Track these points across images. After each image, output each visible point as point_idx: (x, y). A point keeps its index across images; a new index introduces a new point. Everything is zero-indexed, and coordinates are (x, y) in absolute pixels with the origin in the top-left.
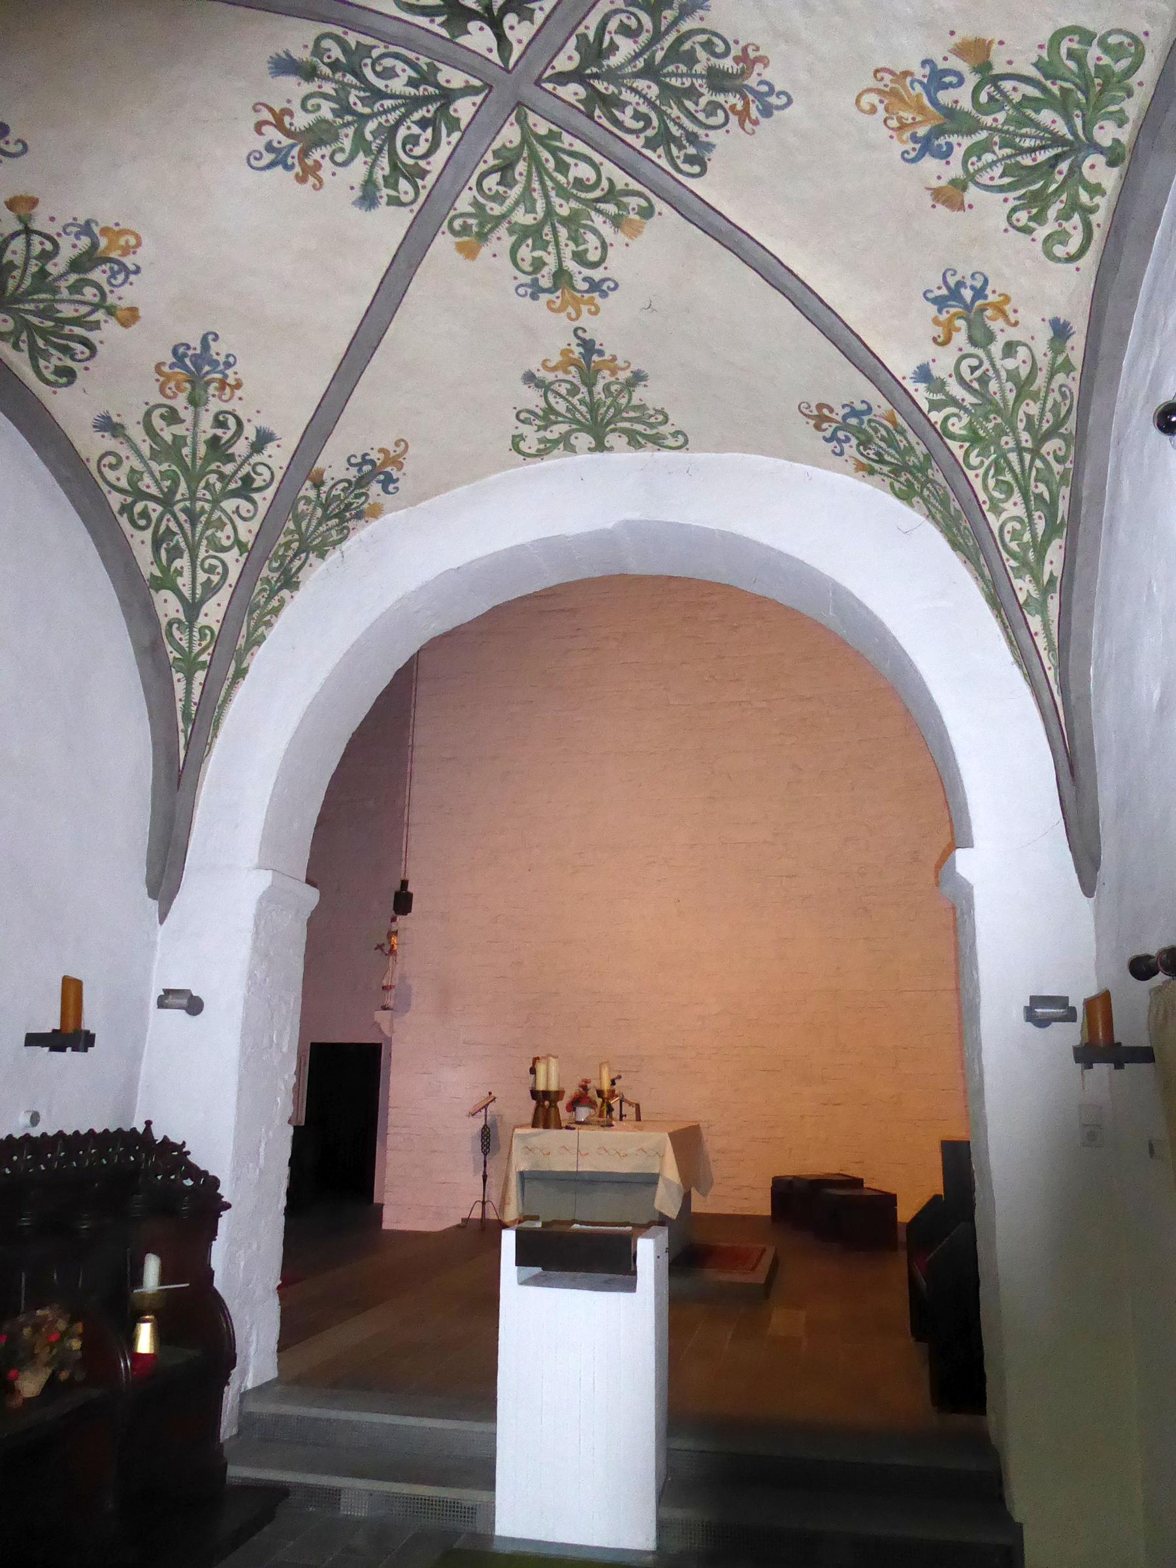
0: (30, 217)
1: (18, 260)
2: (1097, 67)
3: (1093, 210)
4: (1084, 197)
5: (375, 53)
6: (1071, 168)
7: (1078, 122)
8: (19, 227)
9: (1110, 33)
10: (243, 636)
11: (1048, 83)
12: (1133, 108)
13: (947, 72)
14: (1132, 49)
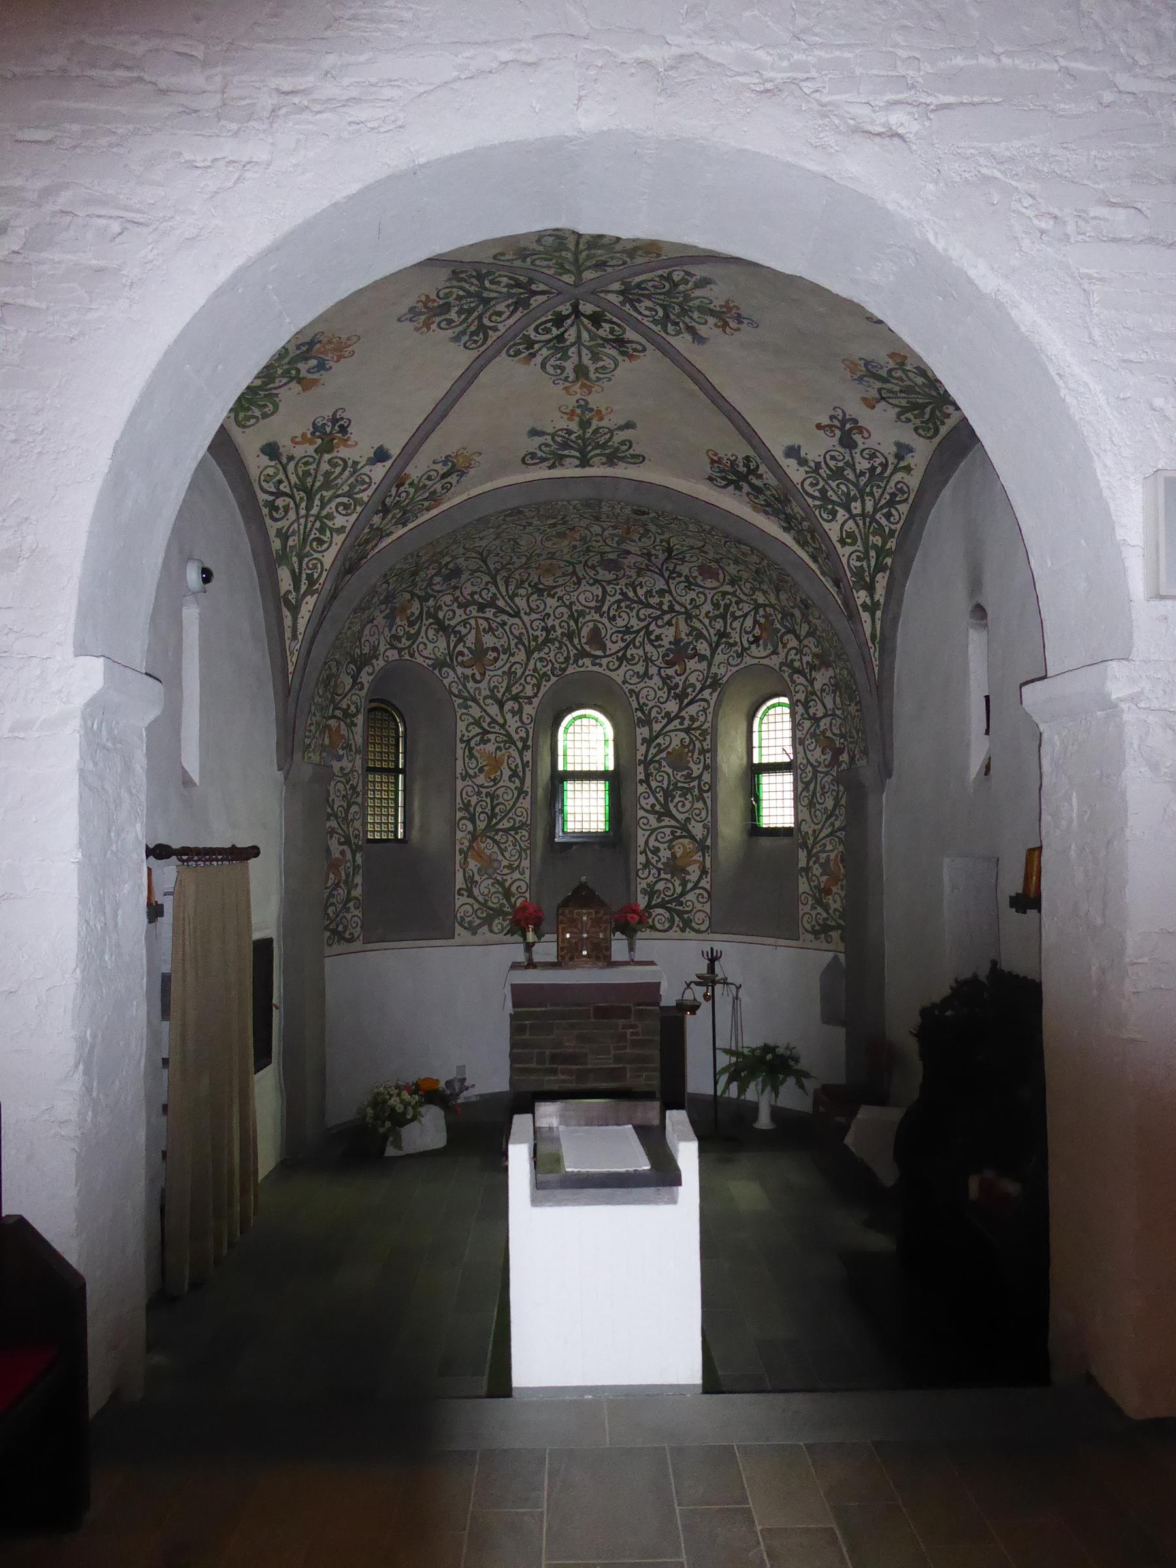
5: (651, 319)
13: (318, 371)
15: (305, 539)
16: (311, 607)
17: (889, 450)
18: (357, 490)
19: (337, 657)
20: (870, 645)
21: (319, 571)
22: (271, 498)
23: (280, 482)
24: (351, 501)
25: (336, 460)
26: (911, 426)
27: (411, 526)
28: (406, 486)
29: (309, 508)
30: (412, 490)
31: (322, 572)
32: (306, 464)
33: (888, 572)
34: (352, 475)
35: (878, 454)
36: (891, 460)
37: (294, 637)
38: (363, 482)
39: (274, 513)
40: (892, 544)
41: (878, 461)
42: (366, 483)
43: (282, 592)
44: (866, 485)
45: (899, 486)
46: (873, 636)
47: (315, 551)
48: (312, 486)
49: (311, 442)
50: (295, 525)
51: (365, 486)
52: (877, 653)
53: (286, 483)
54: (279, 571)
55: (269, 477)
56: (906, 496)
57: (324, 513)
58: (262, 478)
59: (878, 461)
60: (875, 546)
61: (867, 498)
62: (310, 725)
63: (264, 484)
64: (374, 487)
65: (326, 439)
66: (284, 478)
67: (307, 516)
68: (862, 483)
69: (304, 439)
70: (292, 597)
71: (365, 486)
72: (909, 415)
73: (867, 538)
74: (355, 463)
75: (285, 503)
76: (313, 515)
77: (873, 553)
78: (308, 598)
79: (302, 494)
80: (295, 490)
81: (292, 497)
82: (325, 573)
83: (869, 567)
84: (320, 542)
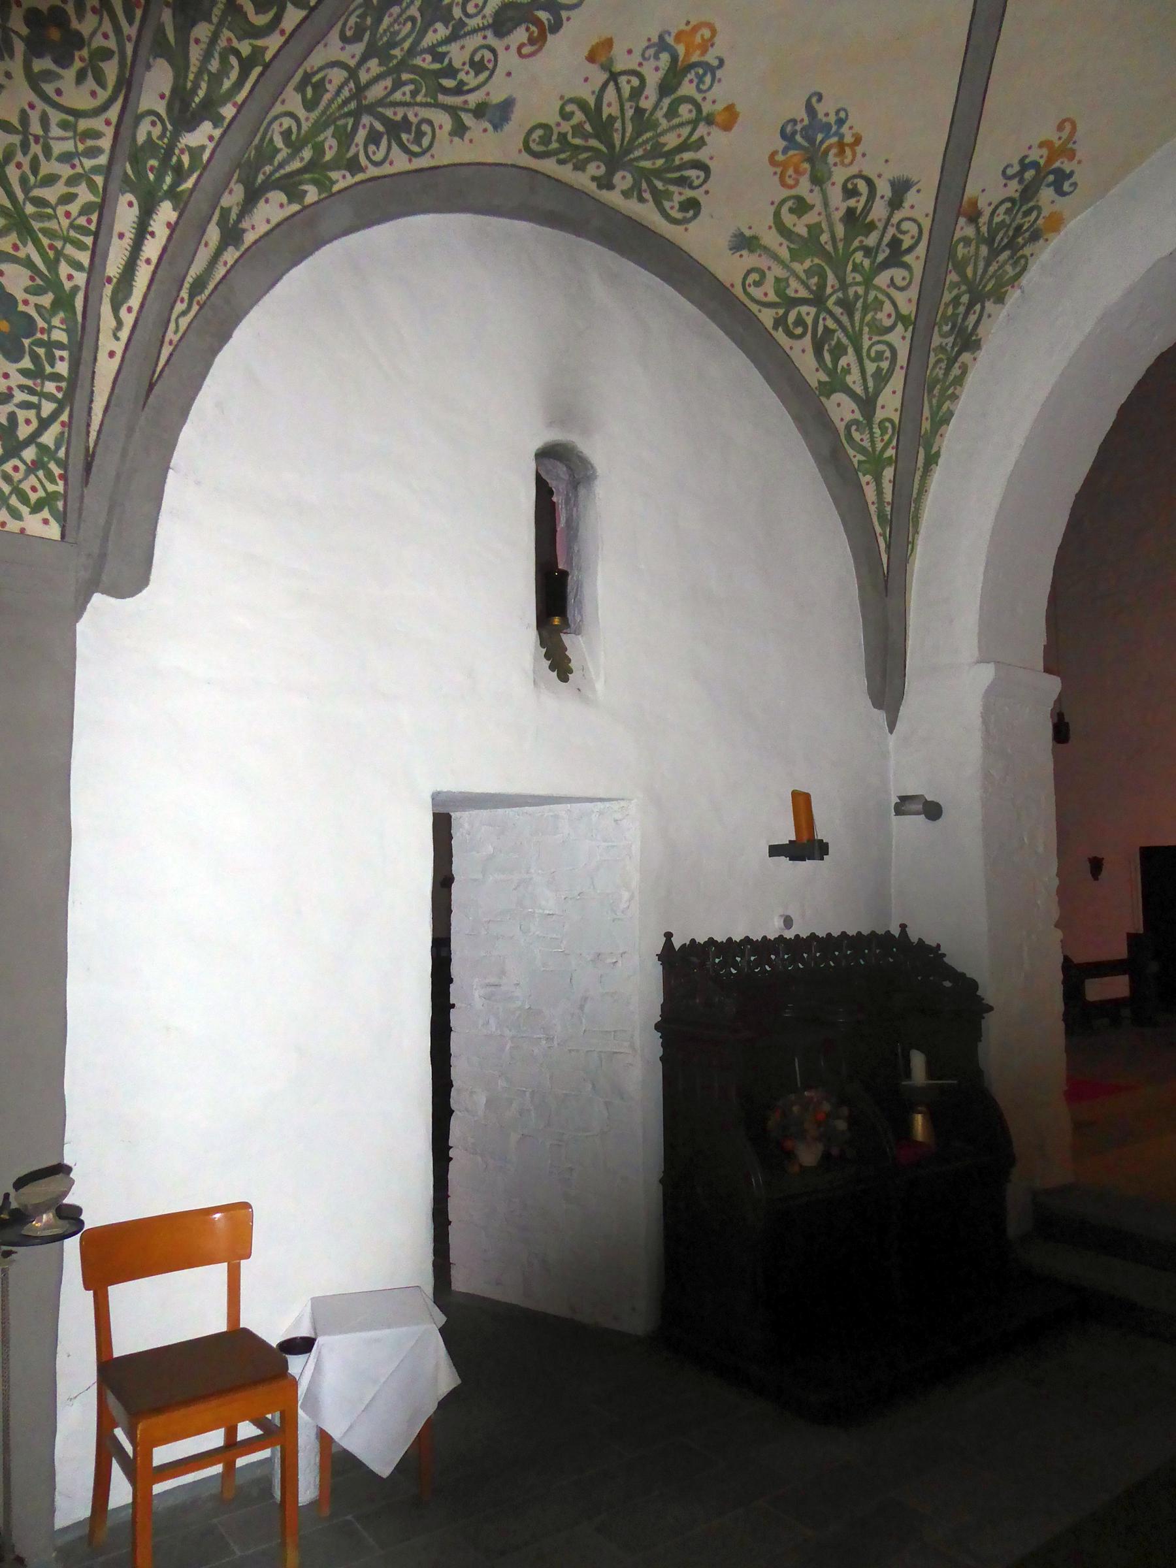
0: (611, 61)
1: (614, 110)
8: (604, 76)
10: (927, 419)
17: (497, 92)
20: (184, 294)
26: (552, 118)
33: (296, 207)
35: (483, 76)
36: (473, 99)
40: (342, 180)
41: (471, 80)
44: (415, 70)
45: (425, 128)
46: (199, 285)
52: (184, 322)
56: (415, 149)
59: (471, 80)
60: (319, 150)
61: (388, 82)
68: (418, 61)
72: (579, 116)
73: (326, 126)
77: (307, 154)
83: (281, 166)
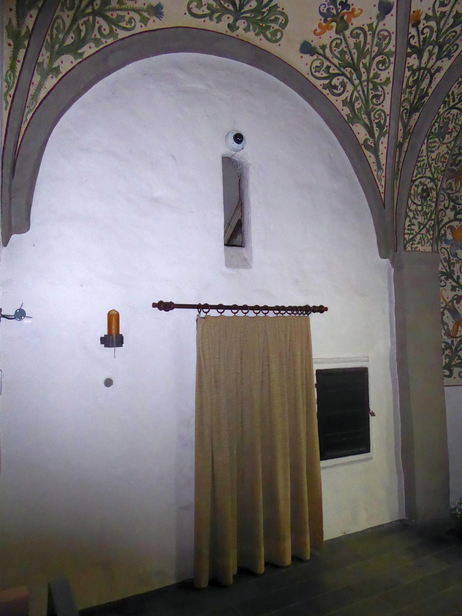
2: (270, 27)
3: (211, 19)
4: (217, 15)
6: (229, 10)
7: (248, 15)
9: (282, 34)
11: (268, 8)
12: (251, 36)
14: (274, 39)
15: (367, 101)
16: (385, 145)
18: (384, 46)
19: (428, 174)
21: (384, 117)
22: (327, 82)
23: (328, 68)
24: (385, 57)
25: (355, 32)
27: (456, 54)
28: (423, 22)
29: (359, 77)
30: (433, 24)
31: (386, 118)
32: (337, 46)
34: (373, 37)
37: (379, 168)
38: (385, 37)
39: (335, 91)
42: (387, 36)
43: (361, 142)
47: (377, 105)
48: (352, 59)
49: (330, 28)
50: (356, 94)
51: (388, 38)
53: (333, 67)
54: (353, 128)
55: (318, 69)
57: (371, 75)
58: (313, 70)
62: (409, 226)
63: (317, 74)
64: (393, 37)
65: (338, 19)
66: (330, 64)
67: (361, 83)
69: (324, 29)
70: (371, 142)
71: (388, 38)
74: (370, 26)
75: (341, 80)
76: (364, 81)
78: (382, 139)
79: (349, 69)
80: (342, 69)
81: (343, 74)
82: (388, 118)
84: (378, 97)
